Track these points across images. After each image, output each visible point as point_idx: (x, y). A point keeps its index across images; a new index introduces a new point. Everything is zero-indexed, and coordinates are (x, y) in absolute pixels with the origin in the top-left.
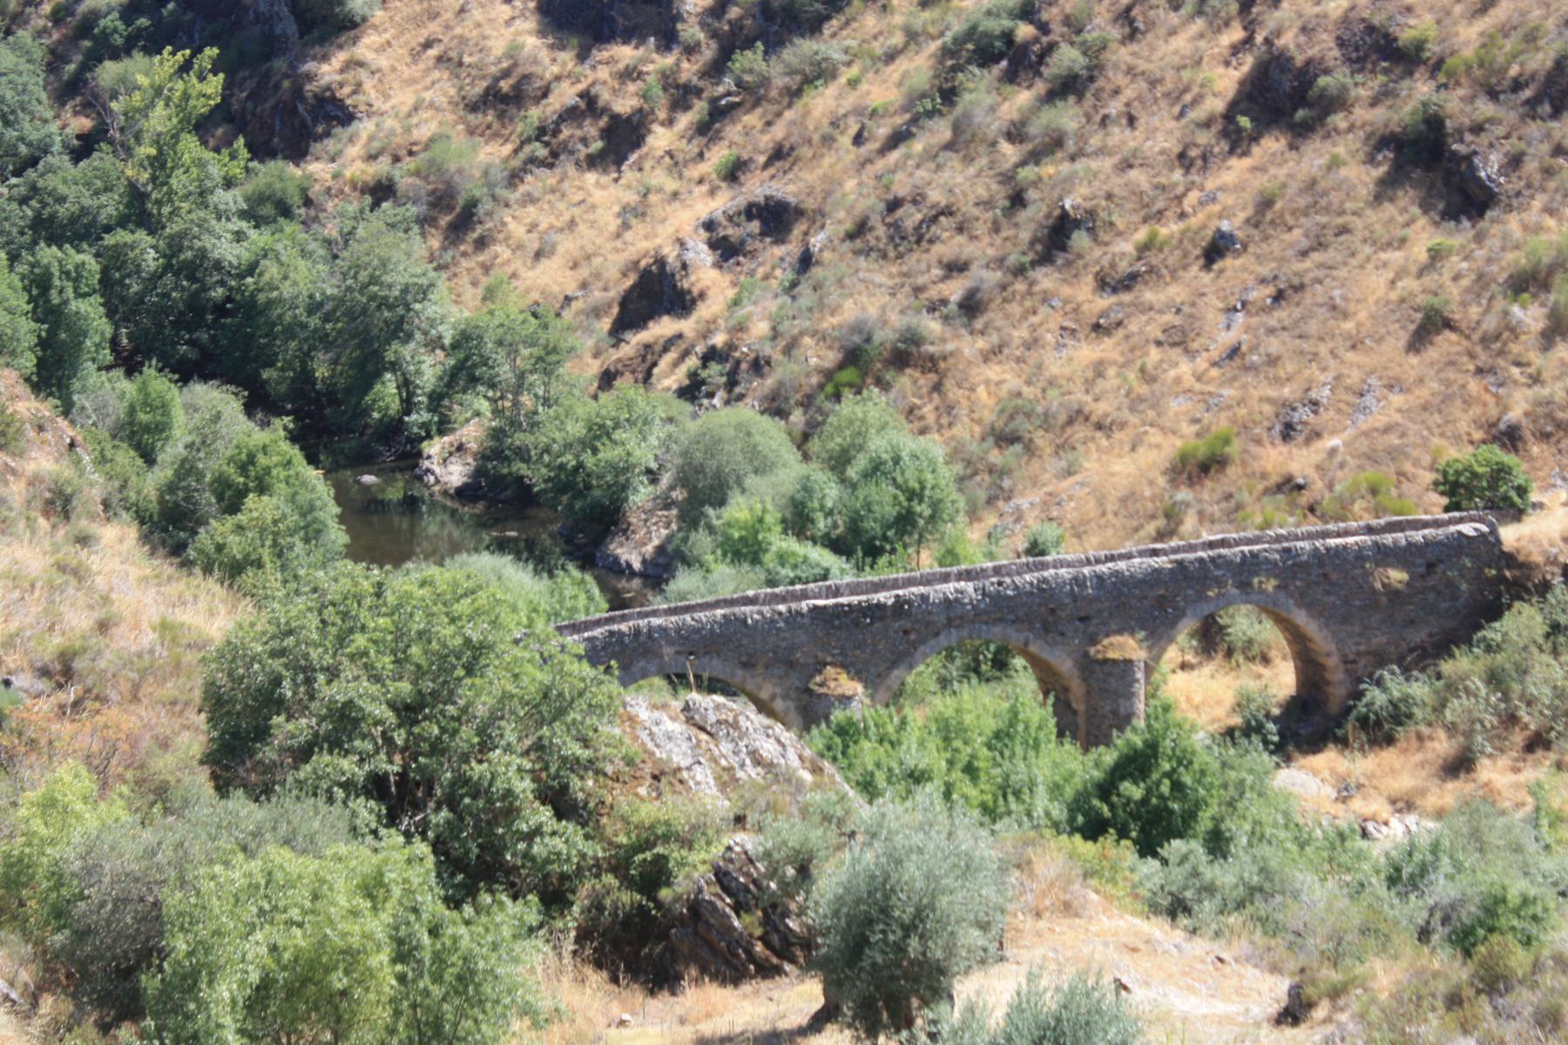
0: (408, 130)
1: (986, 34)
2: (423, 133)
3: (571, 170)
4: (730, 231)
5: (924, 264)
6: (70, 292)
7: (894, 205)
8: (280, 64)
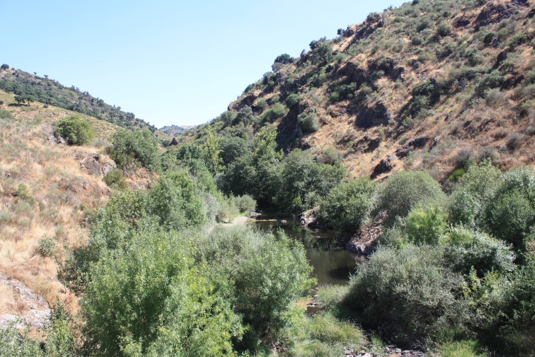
0: (322, 148)
1: (491, 80)
2: (325, 149)
3: (360, 153)
4: (403, 151)
5: (486, 137)
6: (190, 156)
7: (468, 123)
8: (297, 139)
